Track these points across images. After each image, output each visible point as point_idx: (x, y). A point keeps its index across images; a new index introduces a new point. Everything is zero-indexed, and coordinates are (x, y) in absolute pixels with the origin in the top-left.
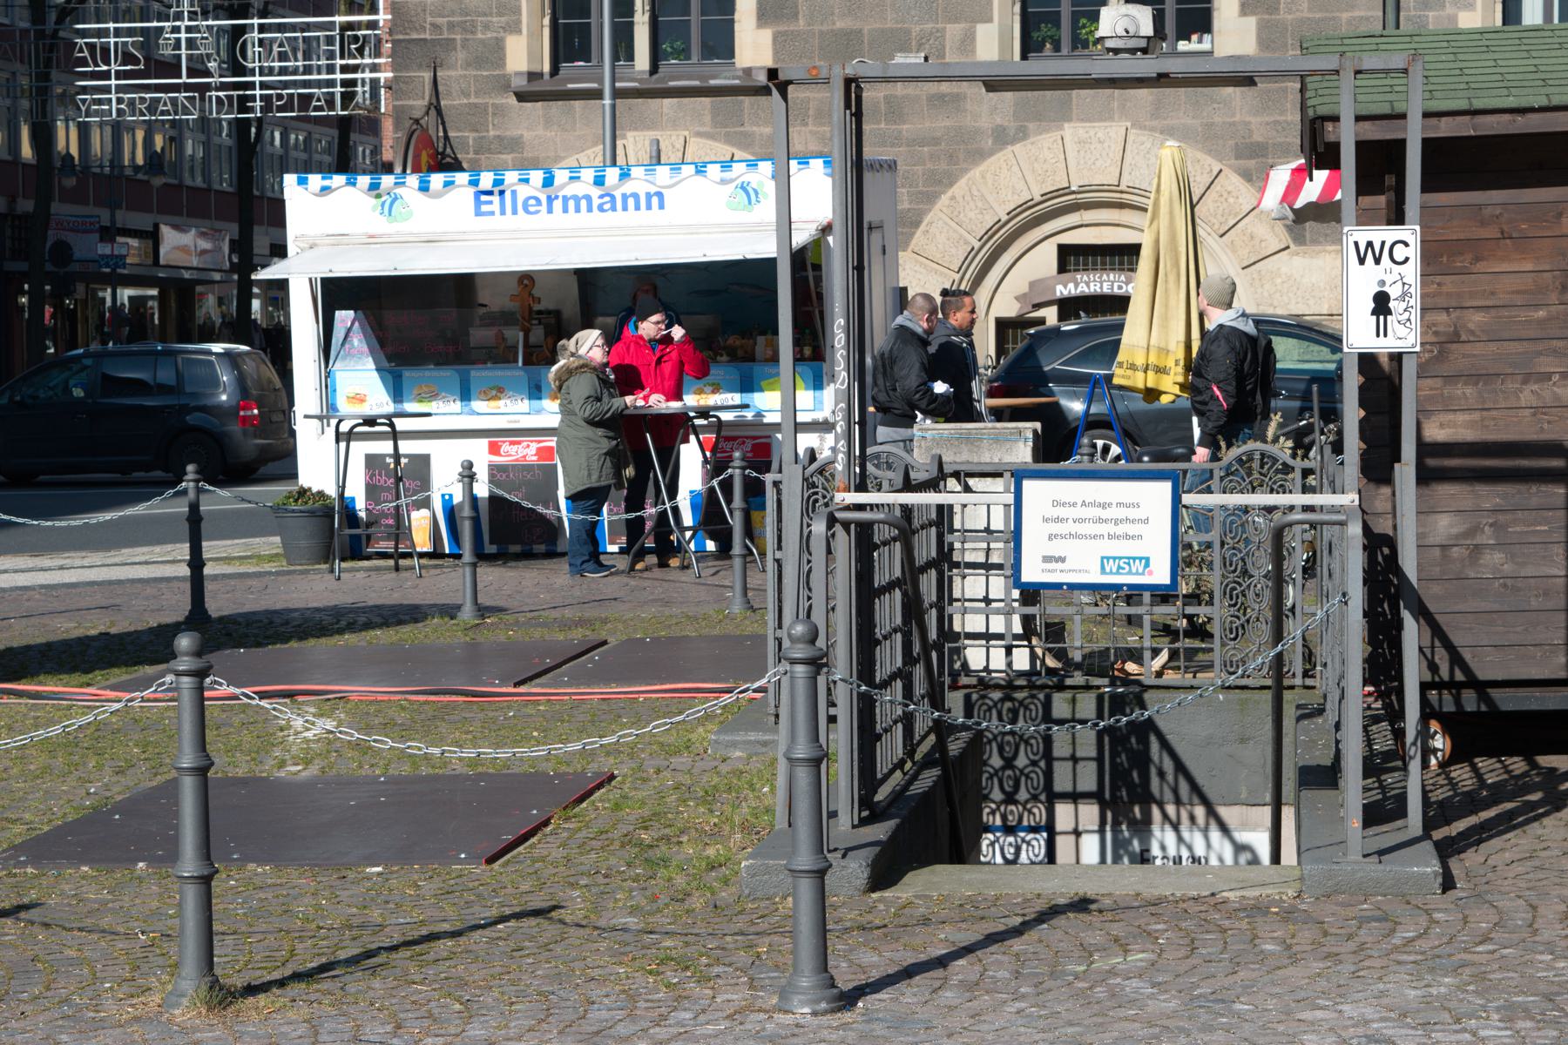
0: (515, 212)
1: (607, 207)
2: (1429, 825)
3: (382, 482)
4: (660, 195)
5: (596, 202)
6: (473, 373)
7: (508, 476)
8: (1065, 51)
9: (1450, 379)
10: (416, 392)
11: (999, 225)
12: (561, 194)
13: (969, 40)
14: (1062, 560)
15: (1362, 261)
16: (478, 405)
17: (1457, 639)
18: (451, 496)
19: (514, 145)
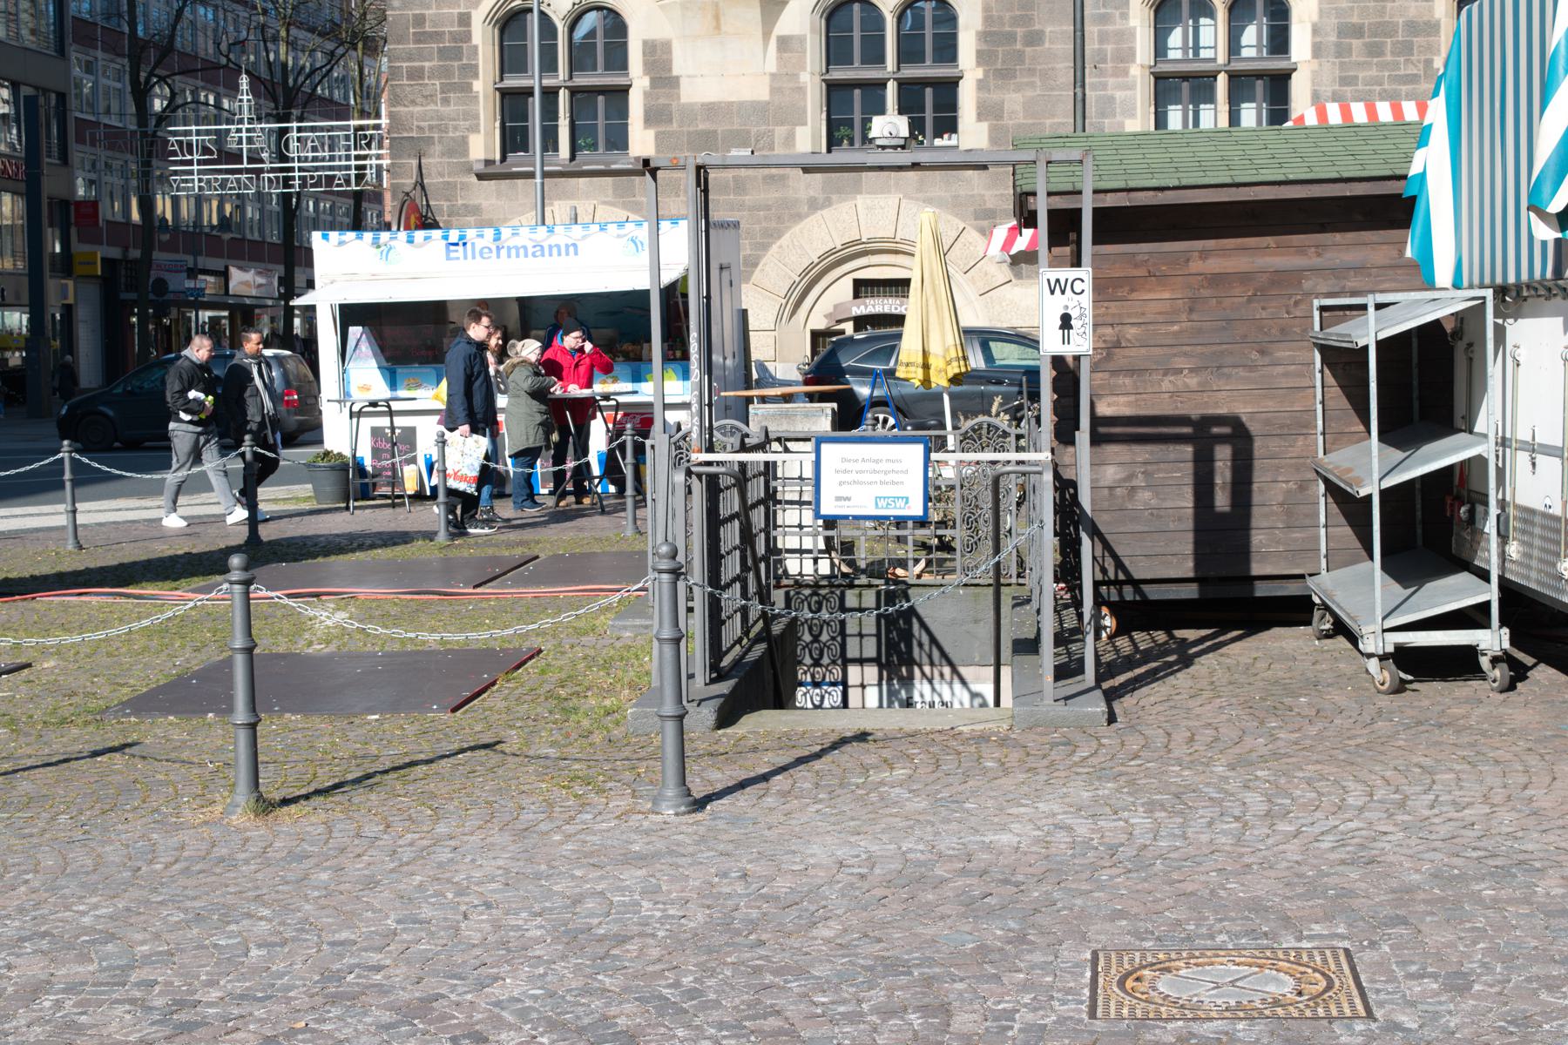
0: (474, 258)
2: (1100, 678)
4: (574, 245)
5: (530, 251)
8: (857, 145)
9: (1115, 373)
11: (813, 265)
13: (790, 139)
14: (848, 499)
15: (1052, 292)
17: (1119, 551)
19: (475, 210)
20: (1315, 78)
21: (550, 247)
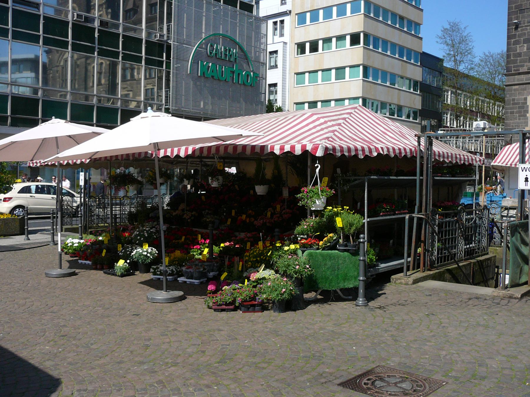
15: (523, 171)
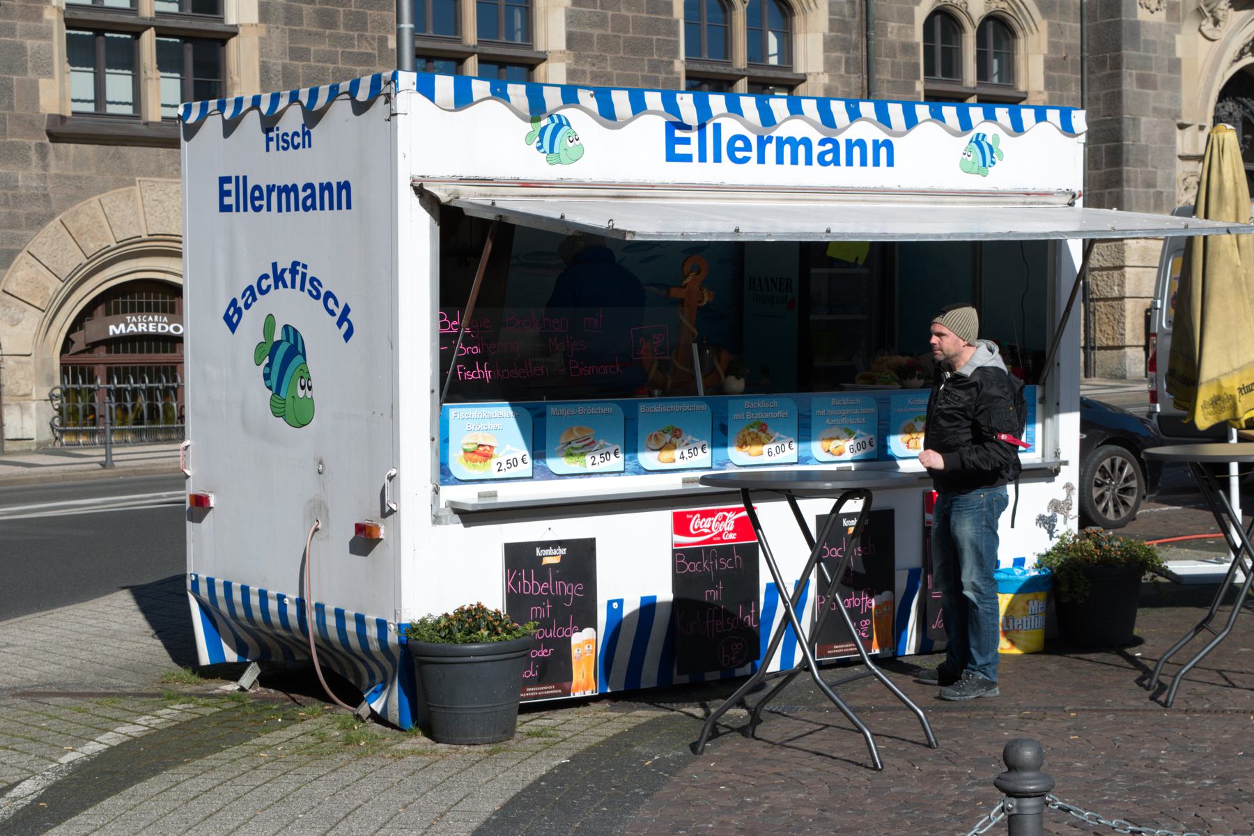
0: (717, 159)
1: (829, 157)
3: (531, 588)
4: (888, 144)
5: (817, 150)
6: (642, 408)
7: (700, 567)
10: (563, 440)
12: (775, 134)
16: (648, 459)
18: (620, 602)
20: (264, 44)
21: (849, 144)
